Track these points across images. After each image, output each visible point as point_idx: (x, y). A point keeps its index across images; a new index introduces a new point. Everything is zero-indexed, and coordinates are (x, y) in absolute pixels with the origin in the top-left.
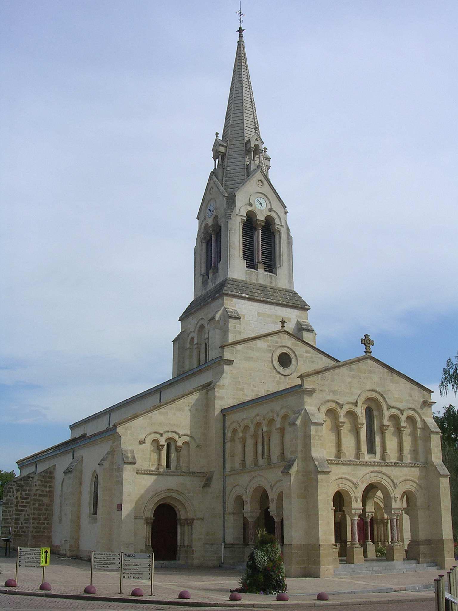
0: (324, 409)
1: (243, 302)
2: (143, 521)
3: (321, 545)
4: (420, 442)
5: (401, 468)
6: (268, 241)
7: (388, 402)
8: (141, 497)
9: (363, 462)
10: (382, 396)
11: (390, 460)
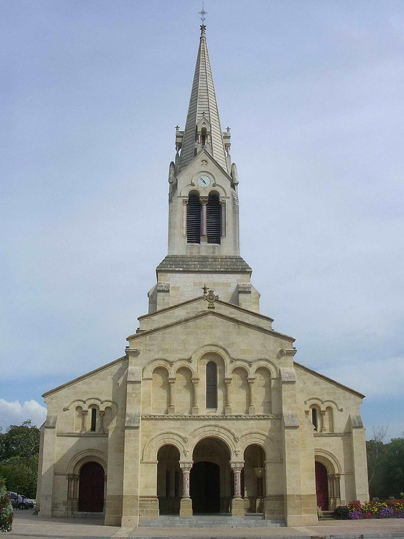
0: (151, 368)
1: (178, 275)
2: (65, 477)
3: (124, 496)
4: (273, 393)
5: (245, 422)
6: (194, 216)
7: (231, 355)
8: (64, 456)
9: (194, 417)
10: (225, 350)
11: (231, 414)
